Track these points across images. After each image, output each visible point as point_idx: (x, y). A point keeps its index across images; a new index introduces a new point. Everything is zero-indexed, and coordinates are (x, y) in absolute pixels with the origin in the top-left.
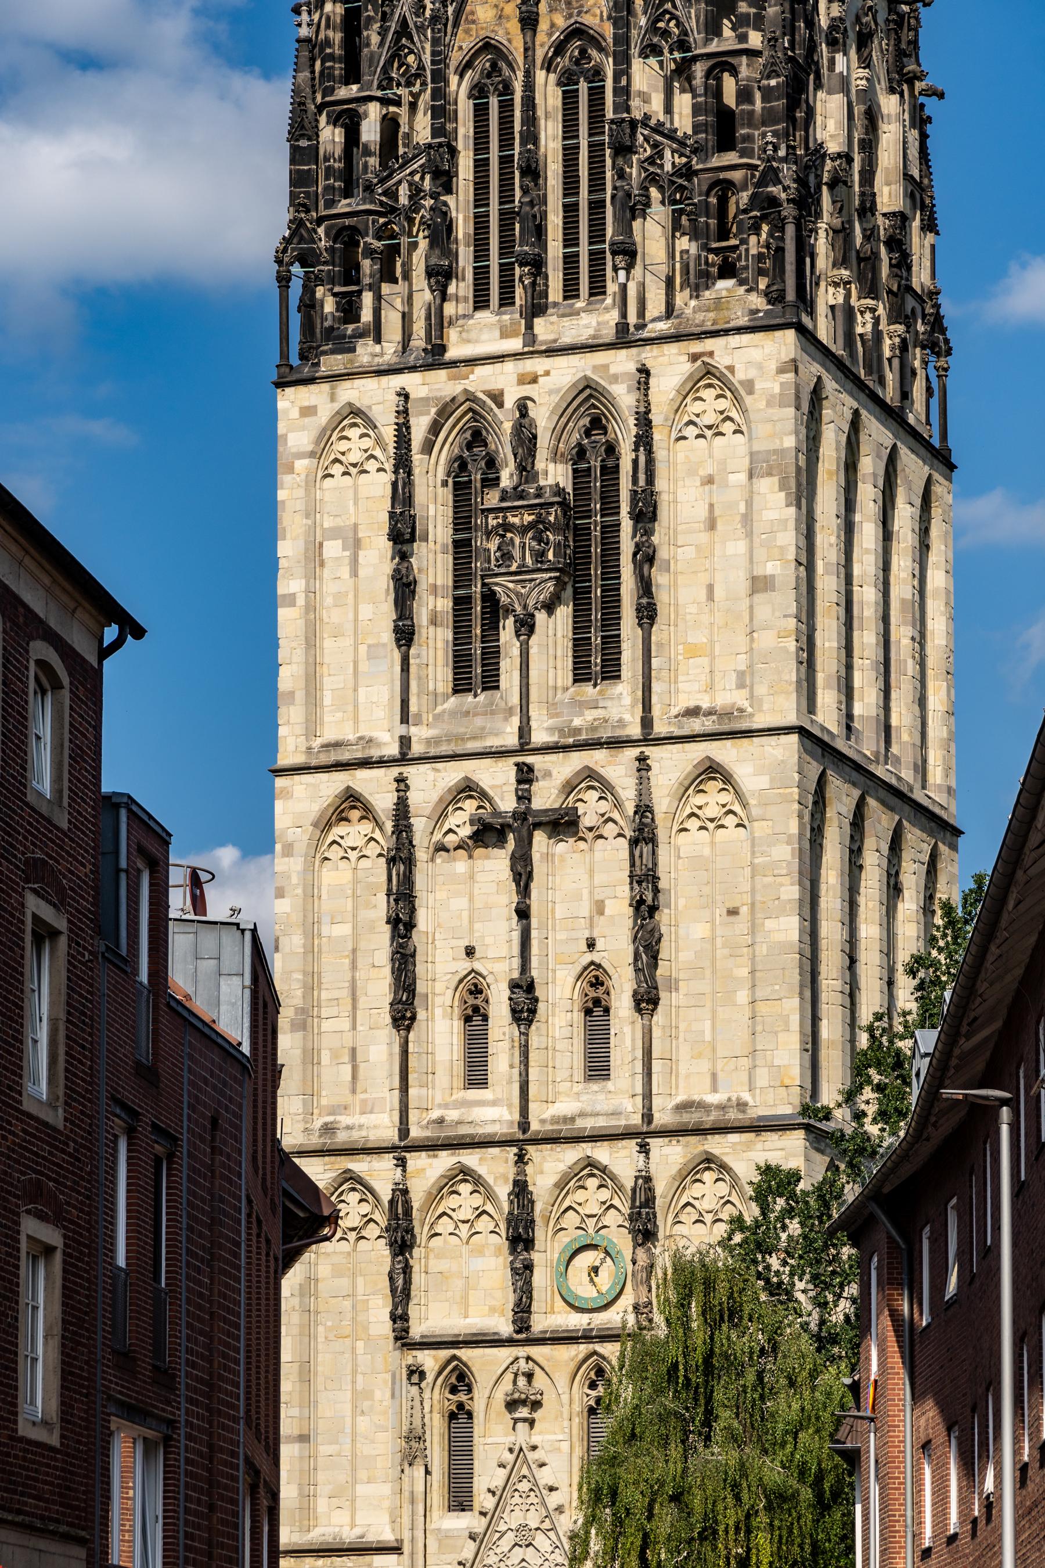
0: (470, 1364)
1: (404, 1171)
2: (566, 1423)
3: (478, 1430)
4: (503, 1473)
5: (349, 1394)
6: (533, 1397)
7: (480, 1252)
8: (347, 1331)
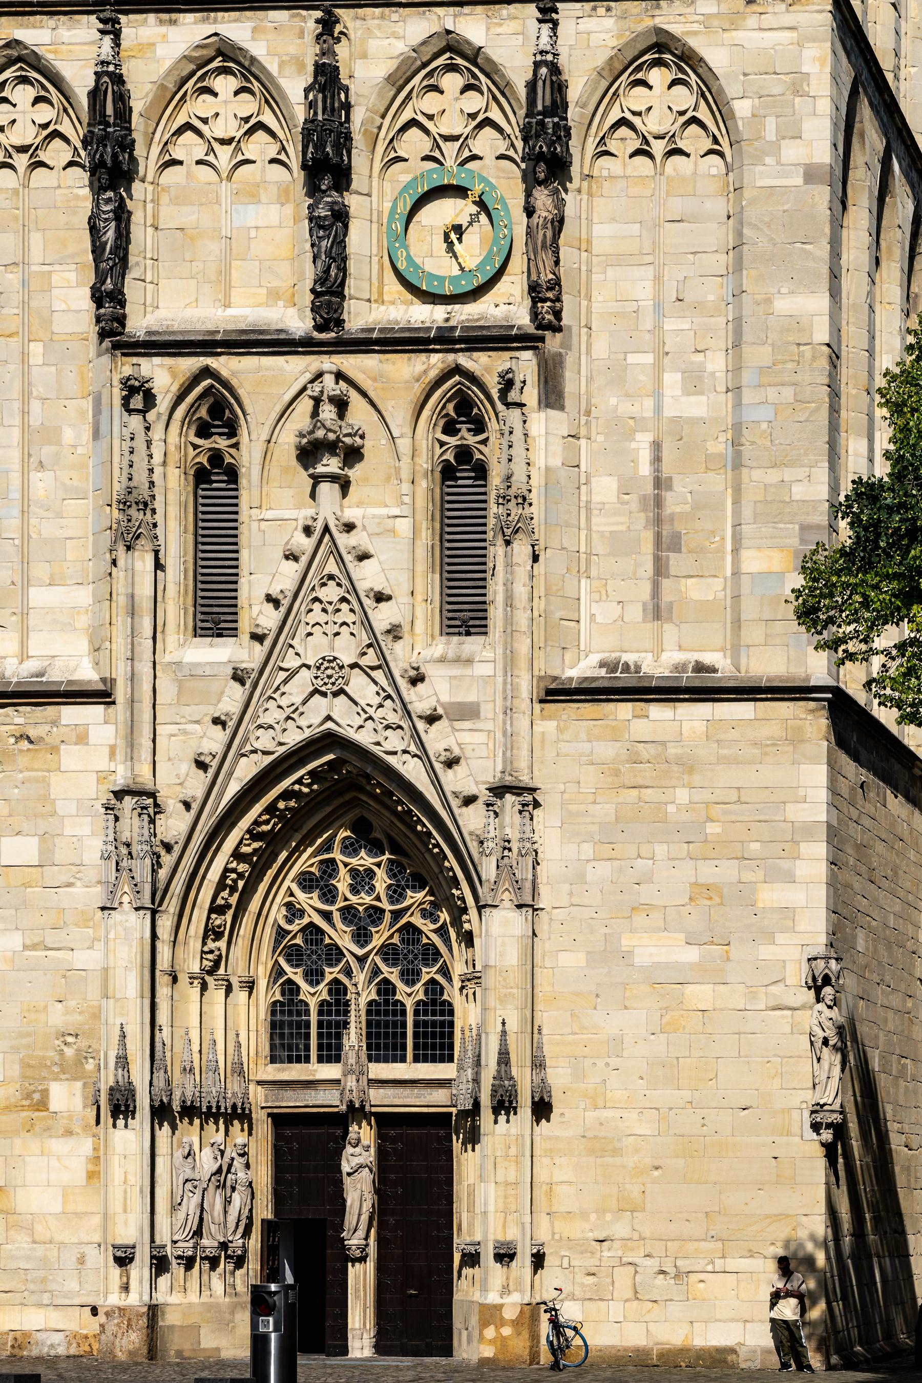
0: (234, 382)
1: (117, 43)
2: (406, 487)
3: (247, 496)
4: (292, 571)
5: (16, 433)
6: (347, 440)
7: (251, 194)
8: (14, 325)
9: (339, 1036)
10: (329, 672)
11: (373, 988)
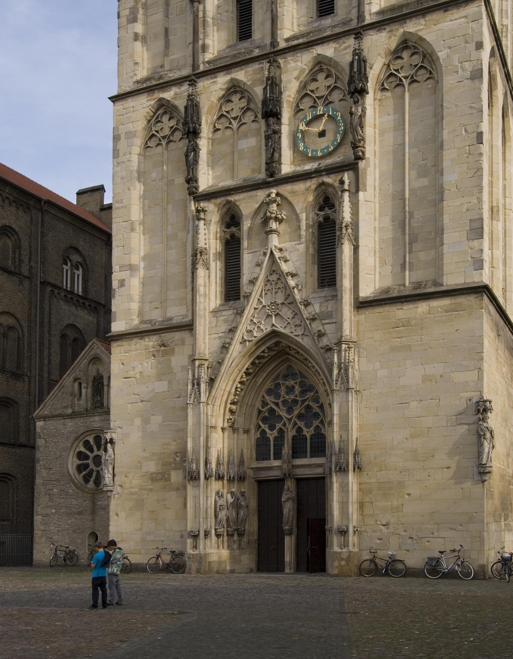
0: (237, 203)
9: (281, 449)
10: (273, 307)
11: (294, 430)
